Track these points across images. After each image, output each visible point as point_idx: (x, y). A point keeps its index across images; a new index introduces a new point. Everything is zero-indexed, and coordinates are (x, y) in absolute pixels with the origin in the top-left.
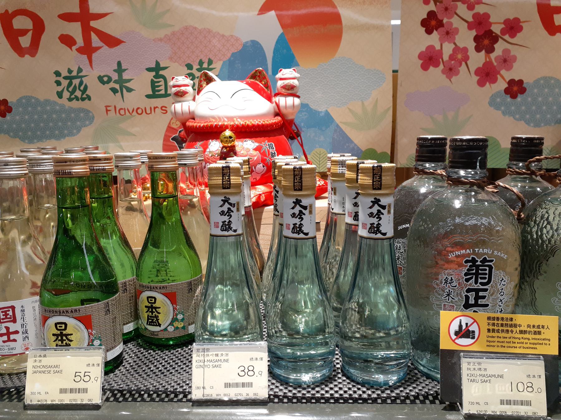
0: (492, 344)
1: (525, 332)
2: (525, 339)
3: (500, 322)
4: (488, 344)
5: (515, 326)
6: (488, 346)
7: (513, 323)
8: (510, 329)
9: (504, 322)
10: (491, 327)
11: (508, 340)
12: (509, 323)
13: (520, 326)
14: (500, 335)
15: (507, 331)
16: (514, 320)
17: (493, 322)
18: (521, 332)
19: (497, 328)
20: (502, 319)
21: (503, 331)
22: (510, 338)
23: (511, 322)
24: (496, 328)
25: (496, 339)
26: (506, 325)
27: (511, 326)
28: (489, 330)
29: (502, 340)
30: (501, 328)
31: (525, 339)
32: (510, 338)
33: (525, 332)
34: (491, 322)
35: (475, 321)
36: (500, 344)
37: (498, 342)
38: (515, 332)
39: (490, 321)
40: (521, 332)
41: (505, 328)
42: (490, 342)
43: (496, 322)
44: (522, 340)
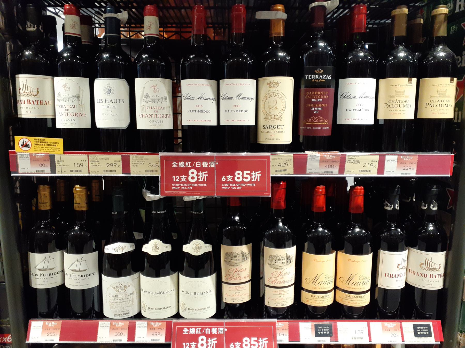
0: (37, 150)
1: (50, 145)
2: (50, 148)
3: (39, 141)
4: (35, 150)
5: (46, 142)
6: (35, 151)
7: (45, 141)
8: (44, 144)
9: (41, 141)
10: (36, 143)
11: (43, 148)
12: (44, 141)
13: (48, 142)
14: (40, 146)
15: (43, 144)
16: (45, 140)
17: (37, 141)
18: (48, 145)
19: (39, 143)
20: (38, 140)
21: (41, 144)
22: (44, 147)
23: (44, 141)
24: (38, 143)
25: (38, 148)
26: (42, 142)
27: (44, 142)
28: (35, 144)
29: (41, 148)
30: (40, 143)
31: (50, 148)
32: (44, 147)
33: (50, 145)
34: (36, 141)
35: (29, 140)
36: (40, 150)
37: (39, 149)
38: (46, 145)
39: (35, 141)
40: (48, 145)
41: (42, 144)
42: (36, 149)
43: (38, 141)
44: (49, 149)
